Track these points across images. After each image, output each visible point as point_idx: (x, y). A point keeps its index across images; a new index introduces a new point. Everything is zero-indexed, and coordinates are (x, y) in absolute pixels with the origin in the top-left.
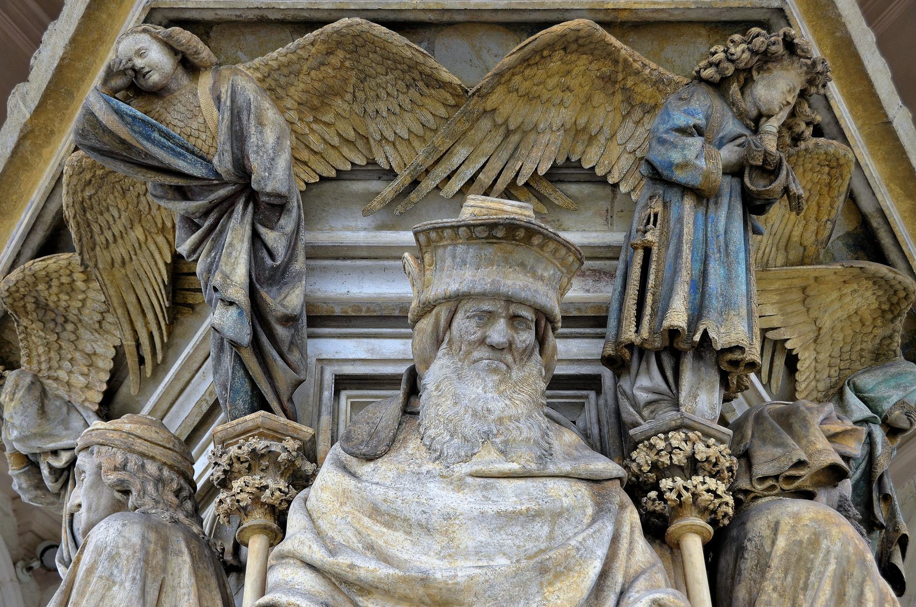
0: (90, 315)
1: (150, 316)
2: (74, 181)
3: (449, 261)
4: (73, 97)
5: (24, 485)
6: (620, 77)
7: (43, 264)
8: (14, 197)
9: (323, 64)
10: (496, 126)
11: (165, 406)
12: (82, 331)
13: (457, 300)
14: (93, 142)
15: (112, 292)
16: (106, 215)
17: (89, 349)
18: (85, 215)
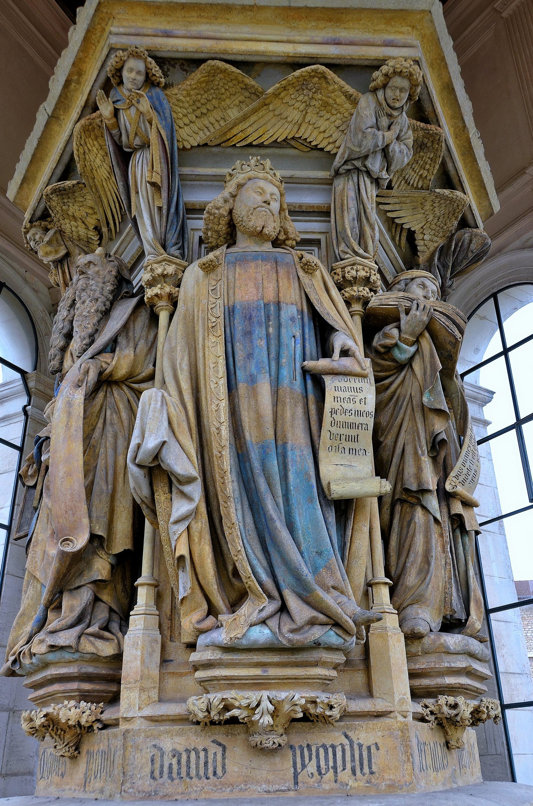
1: (397, 207)
8: (446, 101)
15: (416, 195)
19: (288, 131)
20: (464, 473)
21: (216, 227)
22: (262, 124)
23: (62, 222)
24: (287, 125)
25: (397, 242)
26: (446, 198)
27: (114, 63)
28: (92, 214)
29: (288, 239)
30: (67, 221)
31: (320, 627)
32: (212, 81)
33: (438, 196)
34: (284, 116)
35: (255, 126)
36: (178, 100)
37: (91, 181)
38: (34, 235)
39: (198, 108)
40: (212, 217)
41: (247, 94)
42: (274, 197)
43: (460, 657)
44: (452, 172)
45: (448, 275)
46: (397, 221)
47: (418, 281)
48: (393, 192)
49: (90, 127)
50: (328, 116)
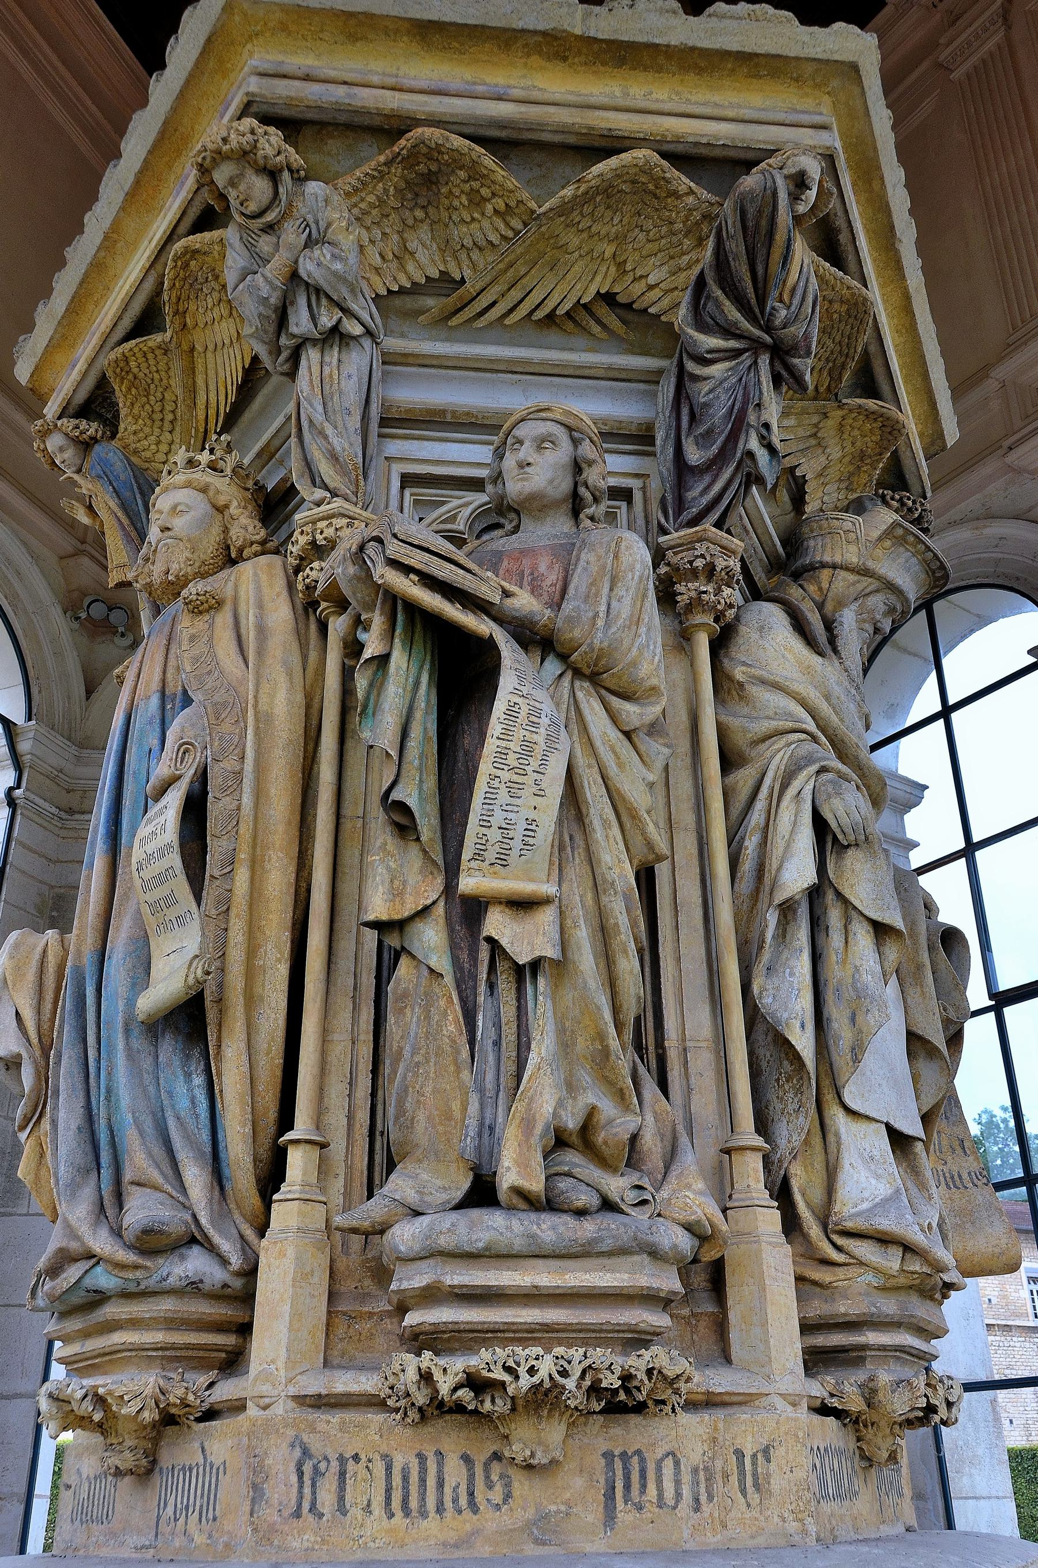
0: (460, 233)
1: (516, 294)
2: (632, 171)
3: (902, 560)
4: (621, 67)
5: (273, 301)
6: (868, 461)
7: (494, 167)
9: (831, 302)
10: (816, 425)
11: (450, 364)
12: (426, 227)
13: (891, 587)
14: (751, 211)
16: (609, 213)
17: (412, 245)
18: (598, 194)
20: (492, 841)
25: (604, 335)
26: (586, 198)
29: (241, 551)
31: (84, 1262)
32: (135, 378)
33: (564, 210)
35: (212, 387)
36: (135, 433)
39: (162, 420)
42: (179, 508)
43: (423, 1265)
44: (571, 140)
45: (733, 314)
46: (540, 314)
47: (510, 441)
48: (471, 287)
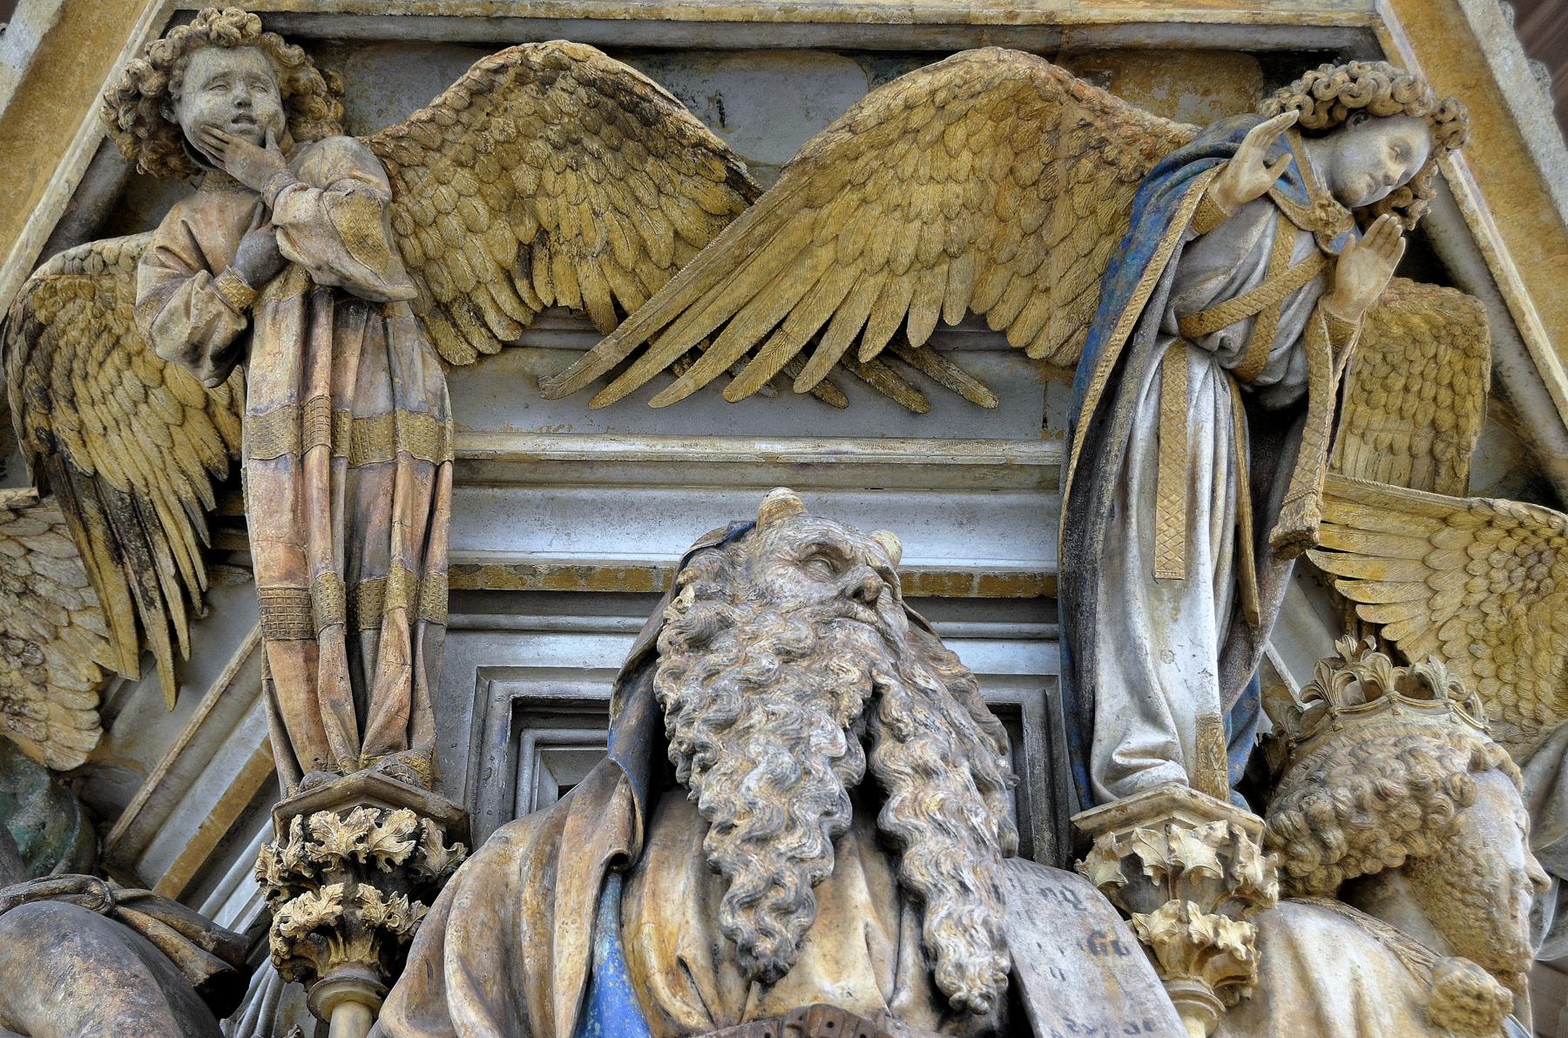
19: (1411, 627)
21: (1387, 840)
22: (1388, 552)
23: (443, 163)
24: (1421, 610)
27: (1386, 91)
28: (618, 266)
30: (463, 178)
34: (1437, 582)
35: (1373, 545)
37: (798, 200)
38: (252, 81)
40: (1417, 810)
41: (1422, 446)
49: (1038, 105)
50: (1486, 668)
